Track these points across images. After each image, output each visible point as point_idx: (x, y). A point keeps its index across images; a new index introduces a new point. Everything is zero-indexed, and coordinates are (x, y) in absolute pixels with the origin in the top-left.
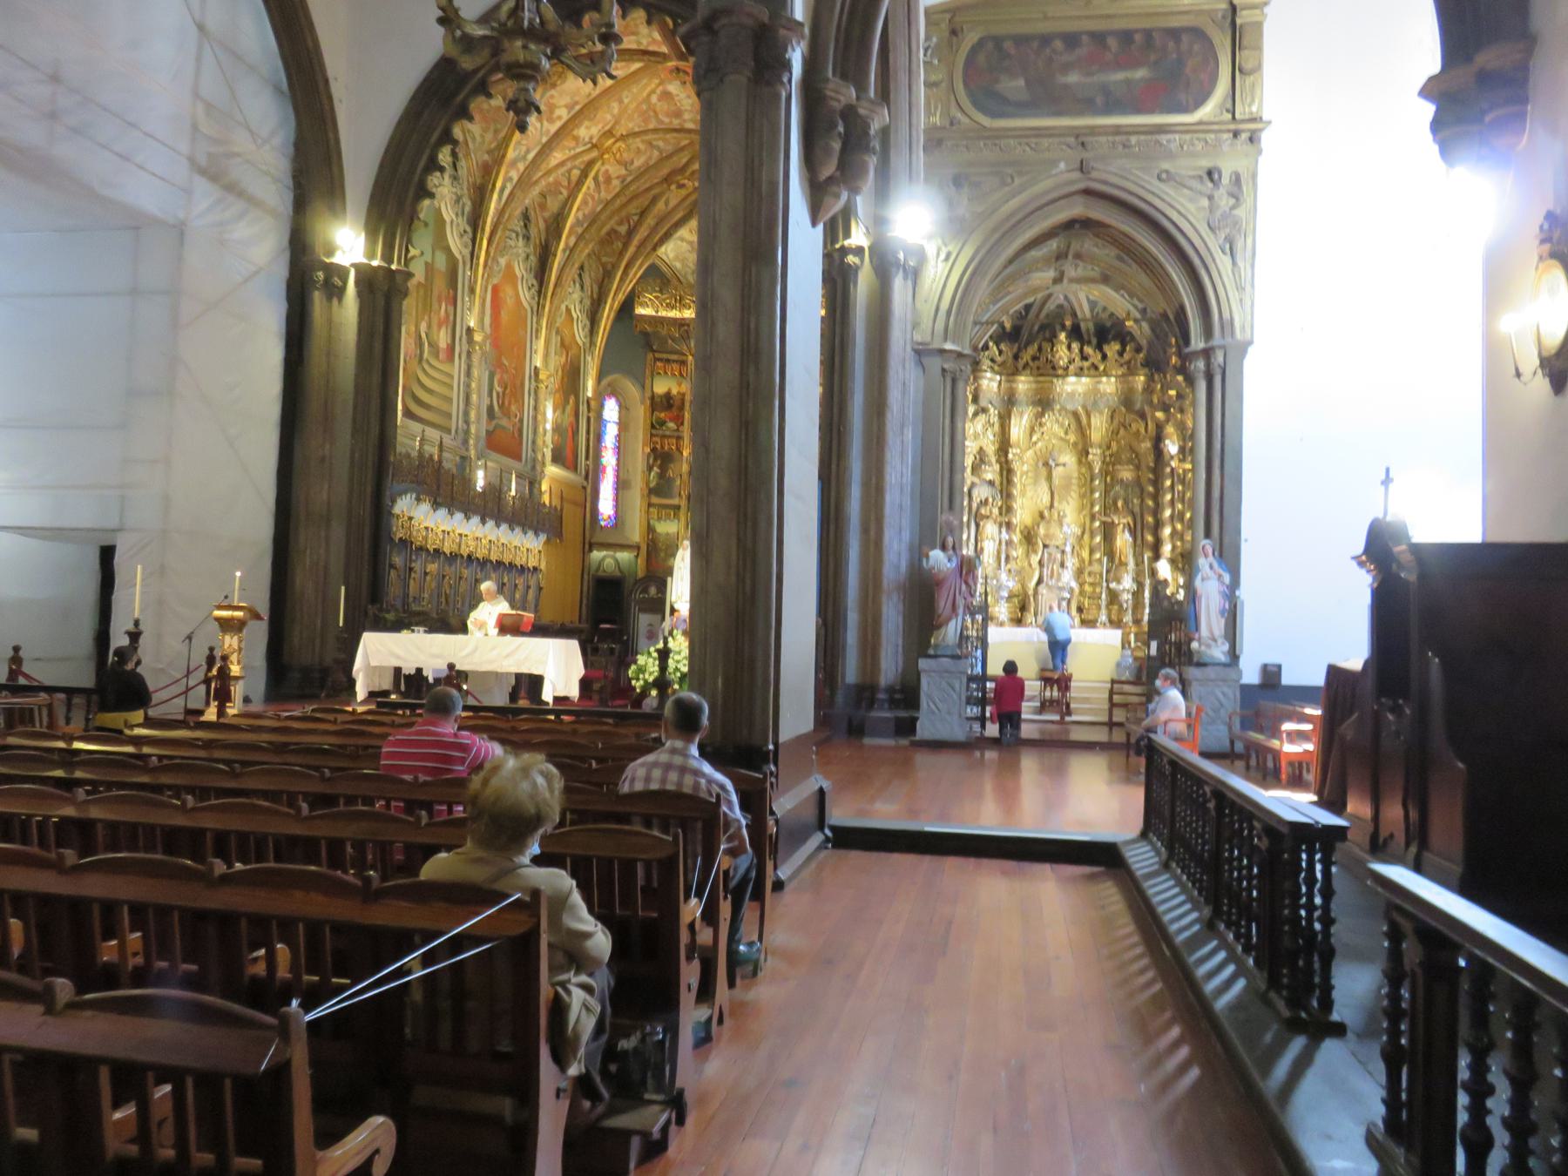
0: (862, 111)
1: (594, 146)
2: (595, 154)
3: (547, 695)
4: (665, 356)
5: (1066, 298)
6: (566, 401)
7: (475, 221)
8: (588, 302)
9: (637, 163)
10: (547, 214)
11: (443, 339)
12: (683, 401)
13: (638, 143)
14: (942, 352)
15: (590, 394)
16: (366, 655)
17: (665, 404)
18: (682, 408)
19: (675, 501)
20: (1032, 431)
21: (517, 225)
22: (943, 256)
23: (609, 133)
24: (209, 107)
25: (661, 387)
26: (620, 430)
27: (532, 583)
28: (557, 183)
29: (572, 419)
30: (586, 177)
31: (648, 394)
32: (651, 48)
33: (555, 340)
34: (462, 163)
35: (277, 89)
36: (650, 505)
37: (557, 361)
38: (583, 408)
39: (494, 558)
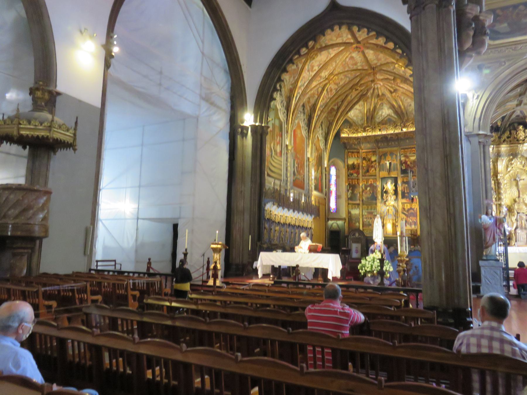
0: (481, 18)
1: (326, 79)
2: (327, 81)
3: (330, 277)
4: (351, 151)
5: (521, 112)
6: (318, 169)
7: (288, 108)
8: (324, 134)
9: (341, 83)
10: (310, 105)
11: (278, 149)
12: (359, 166)
13: (342, 76)
14: (478, 135)
15: (326, 166)
16: (262, 261)
17: (353, 168)
18: (359, 168)
19: (358, 202)
20: (507, 167)
21: (301, 109)
22: (475, 97)
23: (331, 74)
24: (205, 78)
25: (351, 162)
26: (337, 178)
27: (310, 233)
28: (314, 94)
29: (320, 174)
30: (324, 90)
31: (346, 164)
32: (347, 41)
33: (314, 148)
34: (283, 90)
35: (225, 71)
36: (348, 204)
37: (315, 154)
38: (324, 171)
39: (297, 224)
